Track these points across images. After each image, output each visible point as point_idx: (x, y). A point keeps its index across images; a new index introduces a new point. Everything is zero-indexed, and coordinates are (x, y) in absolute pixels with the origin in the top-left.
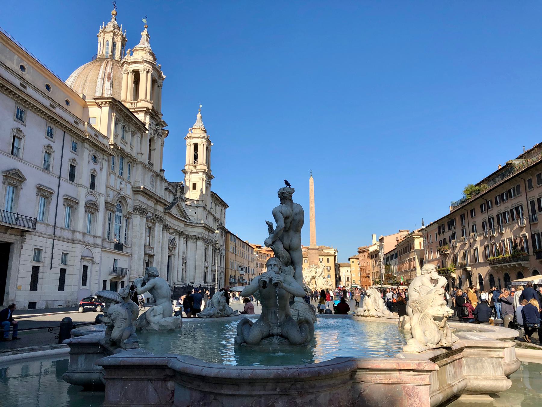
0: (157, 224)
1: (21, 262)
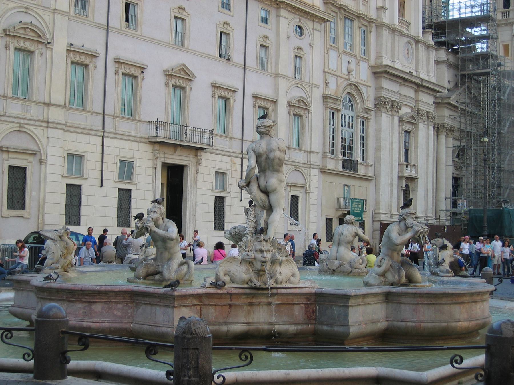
0: (421, 126)
1: (199, 191)
